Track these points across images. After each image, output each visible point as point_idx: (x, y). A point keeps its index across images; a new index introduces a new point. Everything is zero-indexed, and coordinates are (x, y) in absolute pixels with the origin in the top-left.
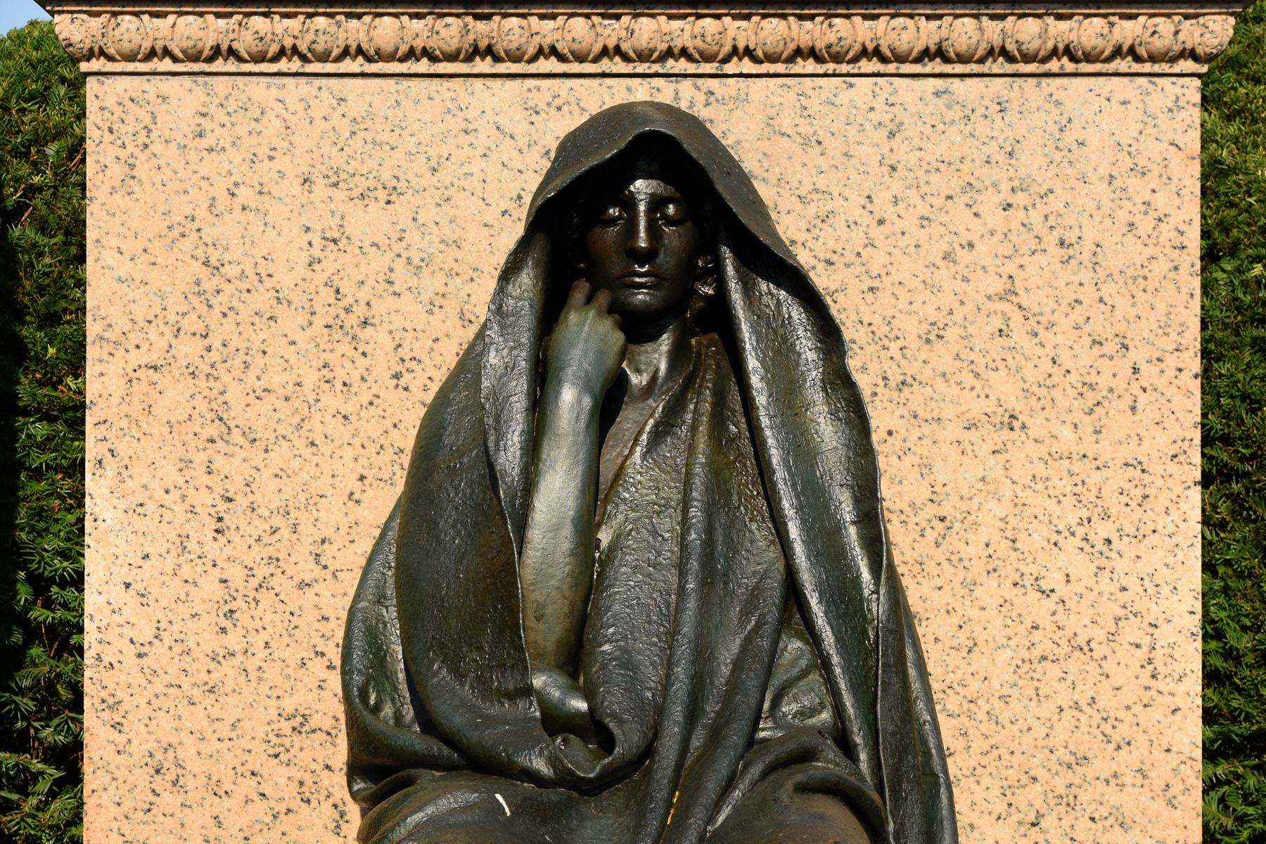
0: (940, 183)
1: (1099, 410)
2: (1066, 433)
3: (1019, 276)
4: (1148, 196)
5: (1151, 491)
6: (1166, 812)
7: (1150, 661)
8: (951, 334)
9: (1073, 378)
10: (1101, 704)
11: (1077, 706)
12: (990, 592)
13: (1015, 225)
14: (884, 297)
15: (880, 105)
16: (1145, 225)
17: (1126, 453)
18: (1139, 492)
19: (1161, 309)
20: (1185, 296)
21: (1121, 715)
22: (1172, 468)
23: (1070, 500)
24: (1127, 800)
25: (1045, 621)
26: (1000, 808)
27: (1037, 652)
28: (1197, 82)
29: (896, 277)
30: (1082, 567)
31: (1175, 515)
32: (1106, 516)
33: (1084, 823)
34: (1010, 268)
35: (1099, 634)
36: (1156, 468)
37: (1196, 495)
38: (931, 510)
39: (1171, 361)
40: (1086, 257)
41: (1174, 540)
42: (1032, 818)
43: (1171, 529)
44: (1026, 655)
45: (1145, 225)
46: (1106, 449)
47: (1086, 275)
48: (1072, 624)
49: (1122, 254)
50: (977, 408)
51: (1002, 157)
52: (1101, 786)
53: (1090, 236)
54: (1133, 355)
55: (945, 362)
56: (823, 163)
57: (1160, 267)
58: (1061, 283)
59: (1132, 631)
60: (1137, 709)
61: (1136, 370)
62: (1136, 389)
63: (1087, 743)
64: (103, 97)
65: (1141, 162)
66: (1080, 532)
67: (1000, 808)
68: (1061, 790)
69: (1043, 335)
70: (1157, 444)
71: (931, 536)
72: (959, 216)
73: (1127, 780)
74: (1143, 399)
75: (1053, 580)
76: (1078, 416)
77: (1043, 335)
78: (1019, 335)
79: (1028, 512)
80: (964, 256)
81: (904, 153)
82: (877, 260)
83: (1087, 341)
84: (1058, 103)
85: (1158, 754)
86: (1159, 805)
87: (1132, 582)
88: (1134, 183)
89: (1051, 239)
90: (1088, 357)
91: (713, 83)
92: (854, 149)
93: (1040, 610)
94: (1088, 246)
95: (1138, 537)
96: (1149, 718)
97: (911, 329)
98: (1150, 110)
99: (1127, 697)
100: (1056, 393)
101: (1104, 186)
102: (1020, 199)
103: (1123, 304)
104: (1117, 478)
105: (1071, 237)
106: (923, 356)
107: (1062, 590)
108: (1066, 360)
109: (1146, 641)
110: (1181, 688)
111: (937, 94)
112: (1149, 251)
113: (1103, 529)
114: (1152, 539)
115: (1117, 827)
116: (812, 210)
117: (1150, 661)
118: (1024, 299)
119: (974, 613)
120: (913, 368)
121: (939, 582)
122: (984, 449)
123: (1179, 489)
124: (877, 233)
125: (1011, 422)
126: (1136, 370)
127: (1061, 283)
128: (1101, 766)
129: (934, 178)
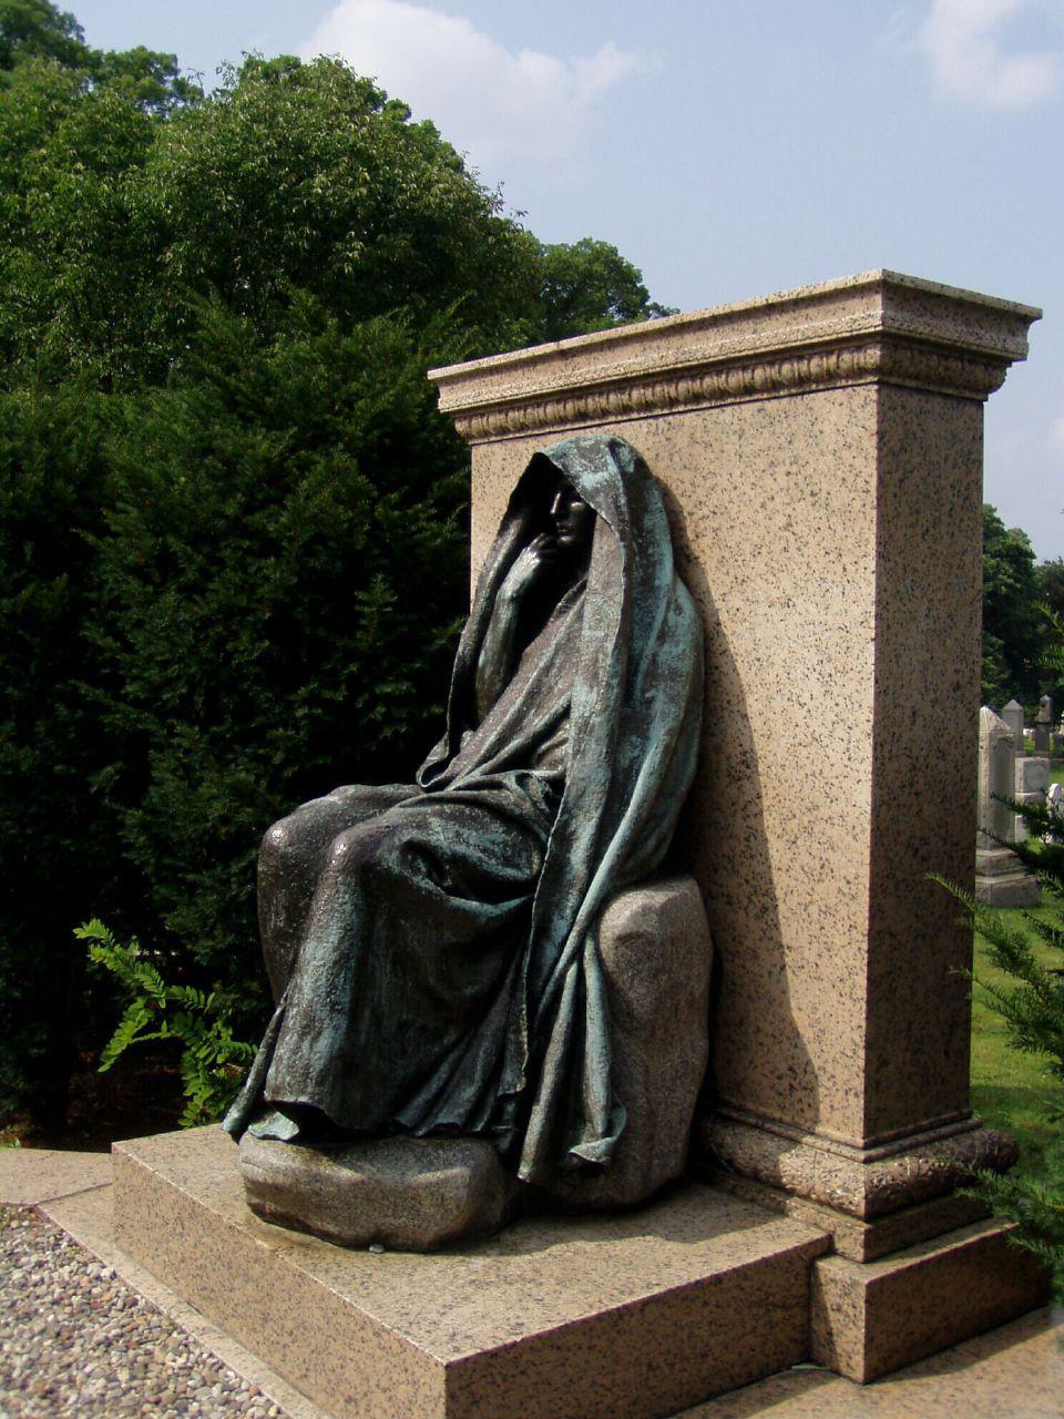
0: (761, 463)
1: (828, 594)
2: (813, 609)
3: (793, 514)
4: (851, 461)
5: (851, 644)
6: (853, 843)
7: (848, 750)
8: (764, 550)
9: (817, 575)
10: (825, 775)
11: (813, 775)
12: (778, 703)
13: (792, 484)
14: (736, 531)
15: (736, 421)
16: (850, 478)
17: (839, 621)
18: (845, 645)
19: (857, 529)
20: (868, 522)
21: (833, 781)
22: (861, 630)
23: (813, 650)
24: (834, 832)
25: (801, 723)
26: (779, 831)
27: (797, 741)
28: (876, 387)
29: (741, 520)
30: (818, 689)
31: (862, 660)
32: (829, 661)
33: (815, 845)
34: (789, 511)
35: (826, 733)
36: (854, 631)
37: (871, 647)
38: (754, 655)
39: (862, 563)
40: (822, 501)
41: (863, 675)
42: (793, 838)
43: (860, 668)
44: (791, 741)
45: (850, 478)
46: (829, 618)
47: (823, 512)
48: (815, 725)
49: (840, 498)
50: (775, 594)
51: (786, 444)
52: (823, 823)
53: (825, 487)
54: (844, 560)
55: (762, 568)
56: (712, 456)
57: (857, 505)
58: (811, 518)
59: (840, 732)
60: (841, 778)
61: (845, 569)
62: (845, 583)
63: (820, 800)
64: (478, 454)
65: (849, 440)
66: (818, 668)
67: (779, 831)
68: (806, 824)
69: (805, 550)
70: (856, 611)
71: (754, 669)
72: (768, 481)
73: (836, 821)
74: (848, 587)
75: (805, 698)
76: (818, 599)
77: (805, 550)
78: (792, 550)
79: (795, 657)
80: (770, 505)
81: (747, 450)
82: (733, 509)
83: (823, 552)
84: (811, 409)
85: (850, 809)
86: (849, 838)
87: (840, 700)
88: (845, 454)
89: (807, 491)
90: (823, 560)
91: (671, 418)
92: (726, 447)
93: (798, 715)
94: (824, 494)
95: (844, 672)
96: (847, 783)
97: (747, 548)
98: (854, 407)
99: (838, 770)
100: (809, 584)
101: (831, 457)
102: (794, 469)
103: (839, 529)
104: (836, 636)
105: (816, 490)
106: (752, 564)
107: (811, 705)
108: (814, 566)
109: (846, 737)
110: (862, 768)
111: (759, 411)
112: (852, 496)
113: (828, 668)
114: (851, 674)
115: (830, 851)
116: (709, 483)
117: (848, 750)
118: (795, 529)
119: (771, 715)
120: (748, 572)
121: (756, 696)
122: (776, 618)
123: (863, 643)
124: (734, 494)
125: (788, 603)
126: (845, 569)
127: (811, 518)
128: (824, 812)
129: (757, 461)
